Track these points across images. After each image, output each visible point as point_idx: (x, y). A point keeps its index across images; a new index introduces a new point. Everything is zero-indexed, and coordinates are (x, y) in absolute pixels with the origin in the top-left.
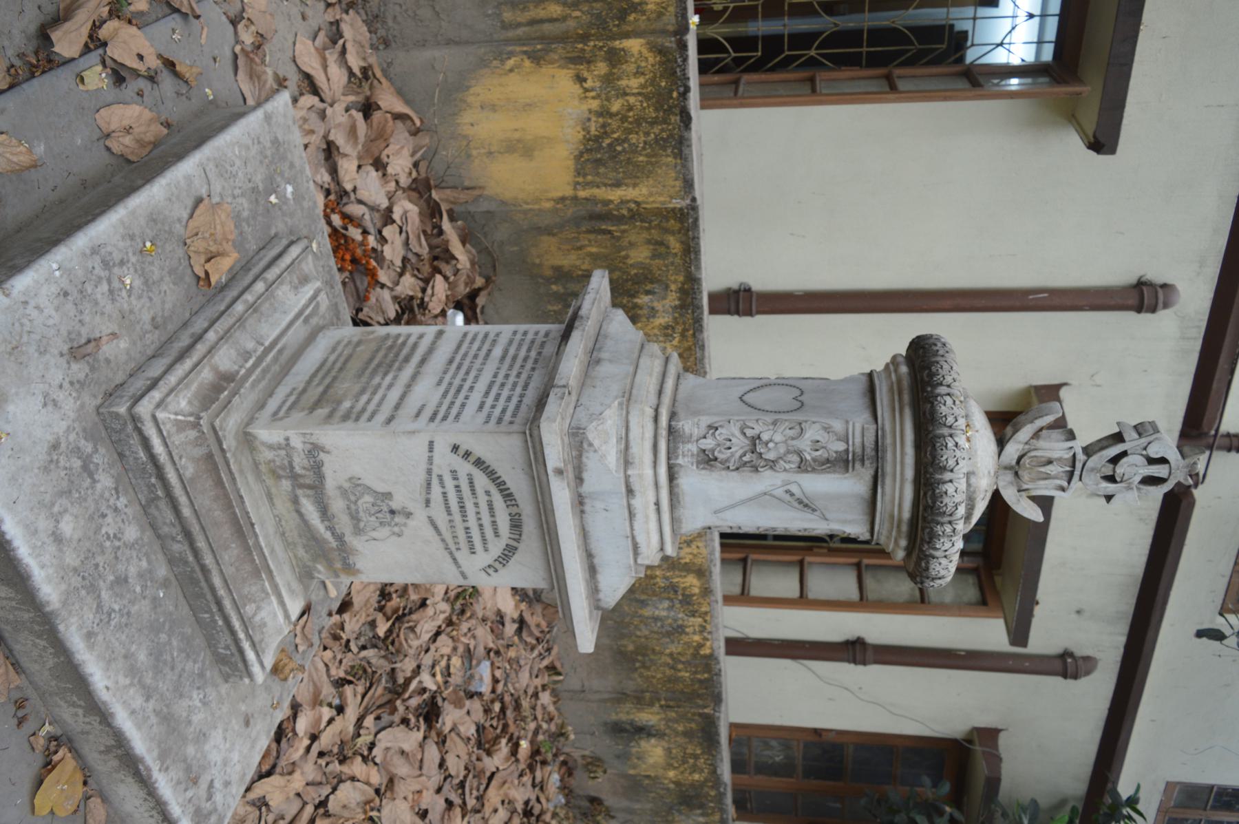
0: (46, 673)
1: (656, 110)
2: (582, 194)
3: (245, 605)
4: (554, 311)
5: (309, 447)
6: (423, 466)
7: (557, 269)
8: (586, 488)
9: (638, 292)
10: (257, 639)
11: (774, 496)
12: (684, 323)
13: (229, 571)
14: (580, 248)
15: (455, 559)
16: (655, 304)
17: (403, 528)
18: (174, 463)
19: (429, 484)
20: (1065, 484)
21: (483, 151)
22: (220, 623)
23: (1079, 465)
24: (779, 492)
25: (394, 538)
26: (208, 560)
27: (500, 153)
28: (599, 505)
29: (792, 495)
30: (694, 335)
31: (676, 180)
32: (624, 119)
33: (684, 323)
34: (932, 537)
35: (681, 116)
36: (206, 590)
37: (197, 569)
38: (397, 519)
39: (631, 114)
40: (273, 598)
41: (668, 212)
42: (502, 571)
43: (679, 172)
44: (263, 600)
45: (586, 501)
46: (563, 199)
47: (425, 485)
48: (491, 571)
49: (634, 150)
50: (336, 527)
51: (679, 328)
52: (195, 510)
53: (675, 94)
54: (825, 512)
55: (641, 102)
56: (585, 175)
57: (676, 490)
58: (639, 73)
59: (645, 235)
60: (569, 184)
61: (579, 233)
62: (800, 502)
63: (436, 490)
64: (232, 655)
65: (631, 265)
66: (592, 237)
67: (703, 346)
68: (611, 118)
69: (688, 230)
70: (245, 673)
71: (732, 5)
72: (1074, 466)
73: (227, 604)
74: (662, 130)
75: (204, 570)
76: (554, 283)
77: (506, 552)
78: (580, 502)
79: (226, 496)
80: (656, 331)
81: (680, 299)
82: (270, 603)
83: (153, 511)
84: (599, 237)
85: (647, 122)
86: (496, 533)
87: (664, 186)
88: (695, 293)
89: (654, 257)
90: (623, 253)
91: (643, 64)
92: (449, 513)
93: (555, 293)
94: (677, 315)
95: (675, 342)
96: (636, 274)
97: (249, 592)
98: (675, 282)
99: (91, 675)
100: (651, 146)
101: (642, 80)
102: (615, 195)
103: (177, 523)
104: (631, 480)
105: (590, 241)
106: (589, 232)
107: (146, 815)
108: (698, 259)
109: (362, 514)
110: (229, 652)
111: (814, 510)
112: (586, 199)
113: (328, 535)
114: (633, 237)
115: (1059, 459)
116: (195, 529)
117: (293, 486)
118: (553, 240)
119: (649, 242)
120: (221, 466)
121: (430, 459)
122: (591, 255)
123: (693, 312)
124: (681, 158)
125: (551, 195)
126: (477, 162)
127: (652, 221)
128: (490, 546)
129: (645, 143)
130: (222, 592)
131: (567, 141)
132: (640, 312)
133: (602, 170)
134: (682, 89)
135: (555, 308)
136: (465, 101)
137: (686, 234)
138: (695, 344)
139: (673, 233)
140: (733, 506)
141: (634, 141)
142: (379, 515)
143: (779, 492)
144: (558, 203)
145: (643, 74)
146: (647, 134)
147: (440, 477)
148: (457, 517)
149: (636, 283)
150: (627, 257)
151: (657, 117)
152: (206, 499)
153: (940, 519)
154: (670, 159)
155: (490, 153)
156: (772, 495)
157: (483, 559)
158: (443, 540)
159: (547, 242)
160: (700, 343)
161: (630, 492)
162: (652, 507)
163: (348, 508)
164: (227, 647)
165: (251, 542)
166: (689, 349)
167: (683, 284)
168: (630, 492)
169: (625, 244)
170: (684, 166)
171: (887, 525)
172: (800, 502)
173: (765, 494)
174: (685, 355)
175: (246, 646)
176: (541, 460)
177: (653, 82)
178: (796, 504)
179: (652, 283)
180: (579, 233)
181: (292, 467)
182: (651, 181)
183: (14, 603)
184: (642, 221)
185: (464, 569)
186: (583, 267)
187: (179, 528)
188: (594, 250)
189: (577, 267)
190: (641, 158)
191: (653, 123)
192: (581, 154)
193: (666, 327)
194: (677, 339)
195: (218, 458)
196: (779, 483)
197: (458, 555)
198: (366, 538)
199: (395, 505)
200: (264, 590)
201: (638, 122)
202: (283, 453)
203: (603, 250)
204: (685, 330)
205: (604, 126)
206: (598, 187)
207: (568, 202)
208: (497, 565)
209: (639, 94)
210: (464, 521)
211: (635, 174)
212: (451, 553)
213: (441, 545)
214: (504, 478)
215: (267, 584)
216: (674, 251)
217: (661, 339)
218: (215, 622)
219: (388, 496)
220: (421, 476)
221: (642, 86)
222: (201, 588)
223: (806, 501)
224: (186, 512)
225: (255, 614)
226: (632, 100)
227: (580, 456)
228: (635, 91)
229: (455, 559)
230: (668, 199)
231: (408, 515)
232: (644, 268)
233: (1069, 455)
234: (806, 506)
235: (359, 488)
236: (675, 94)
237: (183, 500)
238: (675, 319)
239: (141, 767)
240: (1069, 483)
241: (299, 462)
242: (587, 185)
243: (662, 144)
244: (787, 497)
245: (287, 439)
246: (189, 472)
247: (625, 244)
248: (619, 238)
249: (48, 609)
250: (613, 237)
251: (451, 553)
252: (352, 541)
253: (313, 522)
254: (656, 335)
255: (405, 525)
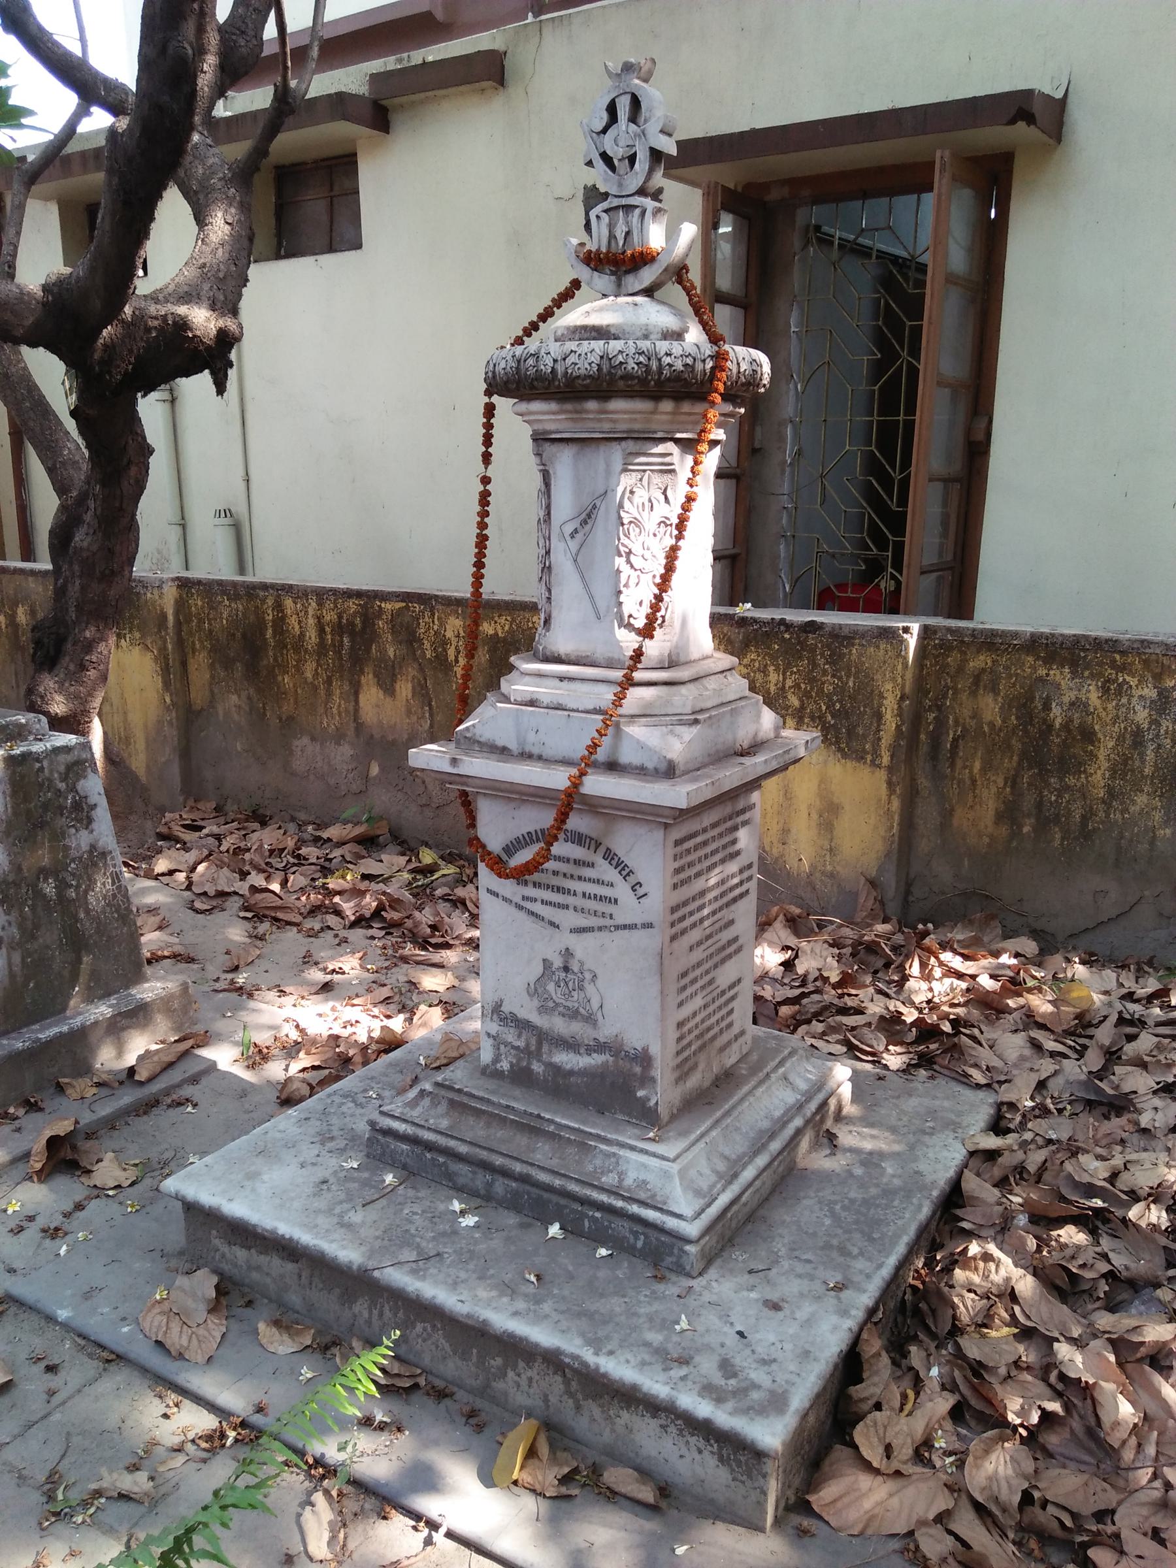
0: (460, 1363)
1: (801, 658)
2: (886, 760)
3: (599, 1179)
4: (1063, 839)
5: (495, 1017)
6: (513, 910)
7: (999, 817)
8: (513, 746)
9: (1045, 721)
10: (642, 1196)
11: (579, 551)
12: (1101, 664)
13: (554, 1163)
14: (974, 782)
15: (625, 927)
16: (1066, 699)
17: (585, 967)
18: (422, 1127)
19: (532, 913)
20: (637, 212)
21: (828, 858)
22: (598, 1215)
23: (616, 202)
24: (573, 545)
25: (599, 982)
26: (518, 1168)
27: (831, 840)
28: (531, 737)
29: (576, 531)
30: (1122, 653)
31: (878, 647)
32: (807, 694)
33: (1101, 664)
34: (539, 376)
35: (810, 632)
36: (555, 1198)
37: (528, 1188)
38: (575, 967)
39: (803, 686)
40: (622, 1152)
41: (937, 663)
42: (640, 876)
43: (869, 642)
44: (617, 1163)
45: (528, 748)
46: (890, 784)
47: (533, 918)
48: (641, 892)
49: (841, 690)
50: (586, 1042)
51: (1109, 672)
52: (470, 1143)
53: (787, 636)
54: (597, 495)
55: (792, 673)
56: (865, 751)
57: (573, 657)
58: (764, 671)
59: (964, 696)
60: (873, 773)
61: (953, 778)
62: (584, 522)
63: (537, 908)
64: (646, 1237)
65: (1004, 721)
66: (959, 763)
67: (1142, 641)
68: (805, 709)
69: (963, 642)
70: (680, 1243)
71: (890, 570)
72: (617, 208)
73: (573, 1187)
74: (822, 655)
75: (524, 1179)
76: (1020, 827)
77: (614, 862)
78: (526, 756)
79: (492, 1115)
80: (1110, 706)
81: (1063, 667)
82: (628, 1161)
83: (461, 1181)
84: (961, 754)
85: (812, 671)
86: (588, 866)
87: (885, 662)
88: (1053, 644)
89: (995, 690)
90: (986, 729)
91: (757, 664)
92: (567, 907)
93: (1035, 830)
94: (1087, 673)
95: (1133, 682)
96: (1017, 718)
97: (596, 1168)
98: (1034, 668)
99: (434, 1297)
100: (837, 670)
101: (771, 668)
102: (890, 722)
103: (477, 1169)
104: (519, 699)
105: (965, 767)
106: (953, 765)
107: (697, 1457)
108: (1003, 634)
109: (569, 1004)
110: (642, 1237)
111: (594, 507)
112: (892, 756)
113: (597, 1059)
114: (966, 713)
115: (611, 227)
116: (484, 1155)
117: (539, 1061)
118: (959, 812)
119: (974, 694)
120: (465, 1100)
121: (505, 899)
122: (984, 770)
123: (1084, 650)
124: (853, 638)
125: (884, 797)
126: (839, 868)
127: (946, 685)
128: (607, 878)
129: (834, 676)
130: (557, 1182)
131: (825, 762)
132: (1076, 723)
133: (860, 731)
134: (782, 628)
135: (1058, 836)
136: (777, 859)
137: (968, 645)
138: (1139, 654)
139: (965, 661)
140: (591, 597)
141: (831, 688)
142: (570, 984)
143: (573, 545)
144: (895, 791)
145: (765, 666)
146: (825, 672)
147: (524, 898)
148: (570, 900)
149: (1031, 719)
150: (992, 725)
151: (808, 659)
152: (476, 1130)
153: (523, 371)
154: (854, 651)
155: (831, 850)
156: (577, 555)
157: (622, 890)
158: (600, 929)
159: (961, 818)
160: (1135, 646)
161: (532, 703)
162: (565, 684)
163: (563, 1015)
164: (636, 1234)
165: (552, 1128)
166: (1146, 663)
167: (1038, 658)
168: (532, 703)
169: (973, 723)
170: (863, 636)
171: (590, 425)
172: (584, 522)
173: (575, 561)
174: (1158, 670)
175: (635, 1209)
176: (458, 779)
177: (774, 658)
178: (588, 527)
179: (1032, 699)
180: (953, 778)
181: (517, 1048)
182: (878, 677)
183: (375, 1312)
184: (945, 697)
185: (639, 921)
186: (1001, 785)
187: (480, 1171)
188: (977, 765)
189: (999, 794)
190: (851, 684)
191: (815, 665)
192: (840, 750)
193: (1105, 690)
194: (1128, 678)
195: (456, 1097)
196: (562, 545)
197: (620, 920)
198: (599, 1014)
199: (558, 962)
200: (609, 1155)
201: (812, 681)
202: (502, 1047)
203: (979, 754)
204: (1113, 664)
205: (813, 718)
206: (879, 739)
207: (894, 779)
208: (632, 880)
209: (784, 674)
210: (575, 894)
211: (868, 694)
212: (617, 927)
213: (604, 935)
214: (524, 831)
215: (603, 1147)
216: (990, 664)
217: (1124, 700)
218: (594, 1220)
219: (547, 964)
220: (522, 915)
221: (777, 670)
222: (550, 1201)
223: (584, 516)
224: (463, 1149)
225: (621, 1180)
226: (789, 683)
227: (479, 742)
228: (781, 678)
229: (625, 927)
230: (901, 660)
231: (568, 953)
232: (1010, 707)
233: (605, 218)
234: (589, 516)
235: (540, 991)
236: (787, 636)
237: (452, 1143)
238: (1092, 676)
239: (567, 1360)
240: (637, 207)
241: (510, 1036)
242: (876, 753)
243: (835, 659)
244: (579, 536)
245: (489, 1035)
246: (444, 1124)
247: (973, 723)
248: (965, 730)
249: (355, 1267)
250: (963, 736)
251: (617, 927)
252: (606, 1032)
253: (581, 1065)
254: (1117, 707)
255: (582, 963)
